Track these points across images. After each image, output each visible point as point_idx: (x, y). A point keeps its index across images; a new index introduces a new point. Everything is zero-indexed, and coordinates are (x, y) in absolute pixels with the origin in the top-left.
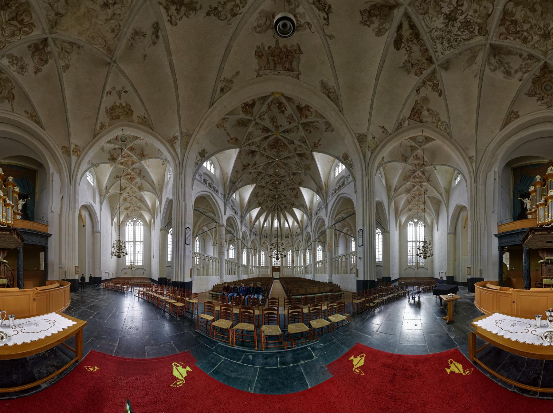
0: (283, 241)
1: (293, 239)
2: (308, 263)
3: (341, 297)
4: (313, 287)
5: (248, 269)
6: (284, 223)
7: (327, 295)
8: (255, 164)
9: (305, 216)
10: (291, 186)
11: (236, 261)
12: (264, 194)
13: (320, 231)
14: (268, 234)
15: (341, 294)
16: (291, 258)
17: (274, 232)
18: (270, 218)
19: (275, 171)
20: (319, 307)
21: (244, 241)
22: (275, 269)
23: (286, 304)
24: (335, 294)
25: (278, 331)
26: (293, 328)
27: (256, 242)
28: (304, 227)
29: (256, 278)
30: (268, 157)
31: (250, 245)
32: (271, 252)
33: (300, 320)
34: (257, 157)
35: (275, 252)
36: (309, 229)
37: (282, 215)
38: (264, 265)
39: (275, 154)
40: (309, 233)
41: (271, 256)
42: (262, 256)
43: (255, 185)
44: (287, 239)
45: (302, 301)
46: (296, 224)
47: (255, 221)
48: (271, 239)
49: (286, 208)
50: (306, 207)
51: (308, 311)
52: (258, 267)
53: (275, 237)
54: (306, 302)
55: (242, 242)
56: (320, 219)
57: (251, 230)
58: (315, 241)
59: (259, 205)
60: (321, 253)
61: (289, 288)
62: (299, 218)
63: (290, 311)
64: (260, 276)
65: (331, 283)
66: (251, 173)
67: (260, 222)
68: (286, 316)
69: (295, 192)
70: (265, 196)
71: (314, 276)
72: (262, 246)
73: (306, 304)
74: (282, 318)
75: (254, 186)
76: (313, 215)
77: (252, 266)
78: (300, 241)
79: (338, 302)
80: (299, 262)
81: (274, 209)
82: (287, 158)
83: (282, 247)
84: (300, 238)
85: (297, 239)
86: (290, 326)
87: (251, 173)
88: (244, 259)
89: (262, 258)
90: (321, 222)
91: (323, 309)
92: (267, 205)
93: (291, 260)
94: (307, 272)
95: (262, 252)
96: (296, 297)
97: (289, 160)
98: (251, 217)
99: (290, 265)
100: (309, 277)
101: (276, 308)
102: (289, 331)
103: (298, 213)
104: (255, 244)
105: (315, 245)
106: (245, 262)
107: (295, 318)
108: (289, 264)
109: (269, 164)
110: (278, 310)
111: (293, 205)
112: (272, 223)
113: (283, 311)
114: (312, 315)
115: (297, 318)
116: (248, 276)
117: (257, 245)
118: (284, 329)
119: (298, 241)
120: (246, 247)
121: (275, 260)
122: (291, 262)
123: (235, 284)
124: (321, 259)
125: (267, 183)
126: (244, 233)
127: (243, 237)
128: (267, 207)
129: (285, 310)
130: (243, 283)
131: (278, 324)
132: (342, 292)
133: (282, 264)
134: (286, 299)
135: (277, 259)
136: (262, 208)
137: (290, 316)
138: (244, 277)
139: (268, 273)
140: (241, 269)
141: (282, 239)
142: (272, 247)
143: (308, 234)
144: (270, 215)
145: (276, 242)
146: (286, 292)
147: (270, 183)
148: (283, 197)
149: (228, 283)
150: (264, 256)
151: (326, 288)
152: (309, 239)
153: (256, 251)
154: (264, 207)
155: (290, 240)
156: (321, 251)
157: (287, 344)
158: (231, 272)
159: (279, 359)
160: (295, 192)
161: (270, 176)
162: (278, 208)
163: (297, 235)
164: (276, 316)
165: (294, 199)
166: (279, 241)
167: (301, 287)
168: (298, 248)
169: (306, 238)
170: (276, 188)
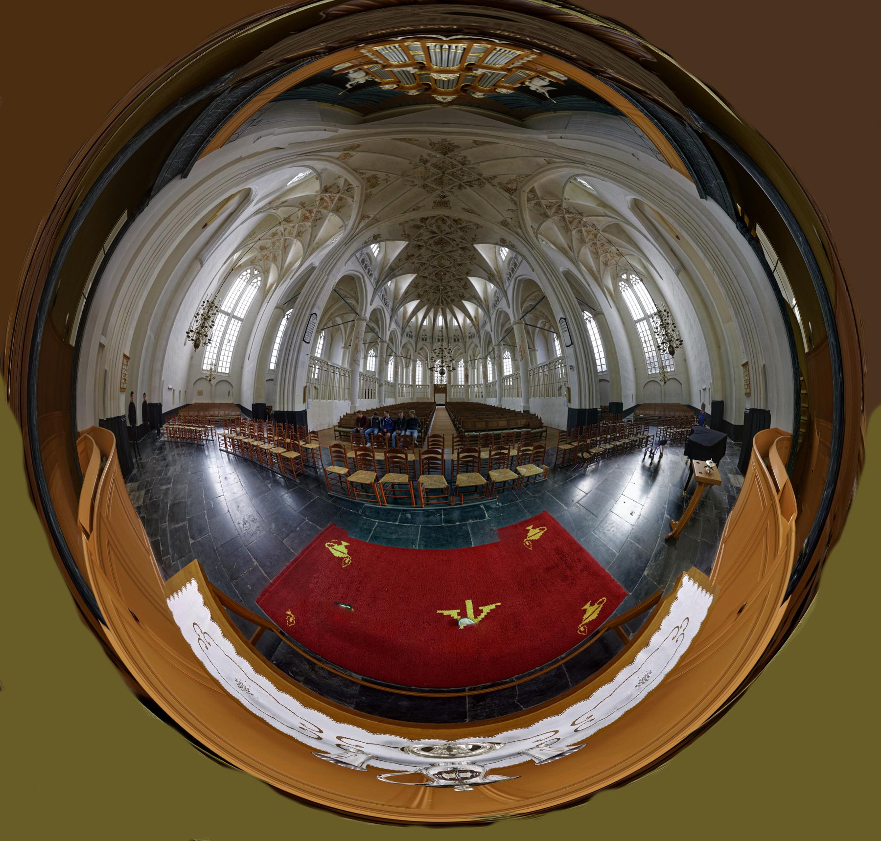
0: (451, 347)
1: (465, 343)
2: (490, 379)
3: (541, 436)
4: (499, 418)
5: (395, 389)
6: (451, 320)
7: (520, 432)
8: (420, 255)
9: (480, 310)
10: (457, 277)
11: (377, 376)
12: (425, 285)
13: (504, 331)
14: (429, 335)
15: (542, 432)
16: (463, 372)
17: (437, 333)
18: (431, 315)
19: (439, 262)
20: (506, 452)
21: (391, 345)
22: (439, 389)
23: (455, 444)
24: (533, 431)
25: (443, 483)
26: (464, 479)
27: (409, 346)
28: (480, 325)
29: (409, 403)
30: (432, 251)
31: (400, 351)
32: (432, 362)
33: (476, 469)
34: (423, 251)
35: (438, 362)
36: (488, 328)
37: (448, 310)
38: (420, 384)
39: (440, 249)
40: (488, 333)
41: (432, 369)
42: (417, 368)
43: (416, 275)
44: (457, 343)
45: (481, 441)
46: (468, 321)
47: (411, 317)
48: (432, 343)
49: (453, 301)
50: (480, 298)
51: (488, 457)
52: (411, 385)
53: (439, 340)
54: (487, 442)
55: (388, 346)
56: (501, 312)
57: (403, 329)
58: (499, 345)
59: (419, 296)
60: (510, 363)
61: (460, 419)
62: (472, 312)
63: (461, 455)
64: (415, 401)
65: (527, 412)
66: (414, 263)
67: (417, 319)
68: (455, 463)
69: (463, 283)
70: (427, 287)
71: (500, 401)
72: (419, 353)
73: (486, 445)
74: (448, 466)
75: (414, 276)
76: (491, 307)
77: (402, 385)
78: (476, 346)
79: (536, 444)
80: (477, 377)
81: (438, 302)
82: (450, 251)
83: (449, 355)
84: (476, 340)
85: (472, 342)
86: (459, 476)
87: (414, 263)
88: (389, 372)
89: (417, 372)
90: (502, 314)
91: (511, 454)
92: (429, 297)
93: (463, 375)
94: (489, 394)
95: (419, 363)
96: (471, 434)
97: (453, 253)
98: (405, 312)
99: (463, 383)
100: (493, 402)
101: (440, 451)
102: (458, 483)
103: (470, 307)
104: (408, 350)
105: (499, 350)
106: (390, 378)
107: (467, 466)
108: (461, 381)
109: (434, 256)
110: (442, 454)
111: (463, 297)
112: (435, 320)
113: (450, 455)
114: (494, 462)
115: (470, 466)
116: (396, 401)
117: (412, 352)
118: (451, 481)
119: (473, 346)
120: (394, 354)
121: (439, 375)
122: (463, 377)
123: (375, 414)
124: (511, 373)
125: (430, 274)
126: (393, 333)
127: (391, 339)
128: (428, 300)
129: (453, 453)
130: (387, 412)
131: (443, 473)
132: (544, 429)
133: (450, 382)
134: (456, 438)
135: (442, 373)
136: (421, 301)
137: (460, 462)
138: (390, 402)
139: (428, 395)
140: (384, 388)
141: (449, 343)
142: (434, 355)
143: (488, 334)
144: (433, 310)
145: (440, 347)
146: (455, 426)
147: (434, 274)
148: (449, 289)
149: (363, 412)
150: (421, 368)
151: (519, 421)
152: (490, 342)
153: (409, 360)
154: (424, 300)
155: (460, 344)
156: (510, 360)
157: (455, 499)
158: (368, 394)
159: (443, 517)
160: (463, 283)
161: (434, 267)
162: (442, 301)
163: (470, 337)
164: (440, 462)
165: (463, 290)
166: (445, 345)
167: (479, 418)
168: (474, 356)
169: (486, 340)
170: (441, 279)
